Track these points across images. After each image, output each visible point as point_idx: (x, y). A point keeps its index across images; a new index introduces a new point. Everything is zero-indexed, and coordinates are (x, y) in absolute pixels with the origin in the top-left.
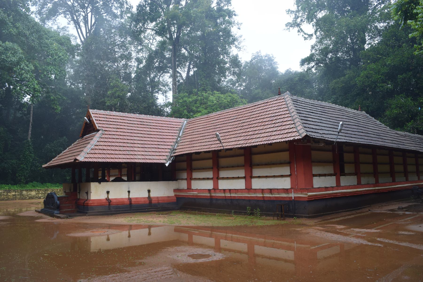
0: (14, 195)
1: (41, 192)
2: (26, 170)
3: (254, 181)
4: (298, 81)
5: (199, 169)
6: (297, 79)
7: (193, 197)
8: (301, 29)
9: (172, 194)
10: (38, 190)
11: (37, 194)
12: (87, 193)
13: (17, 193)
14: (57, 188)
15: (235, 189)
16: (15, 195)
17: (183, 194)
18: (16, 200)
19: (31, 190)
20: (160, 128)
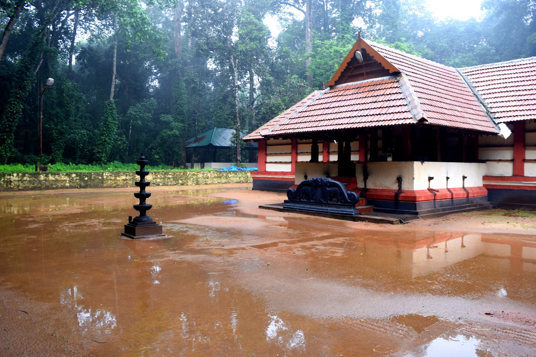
0: (124, 180)
1: (159, 176)
2: (109, 144)
4: (464, 32)
6: (462, 29)
9: (480, 183)
11: (154, 179)
12: (399, 180)
13: (128, 178)
14: (180, 170)
16: (126, 180)
17: (510, 184)
18: (127, 187)
20: (442, 77)
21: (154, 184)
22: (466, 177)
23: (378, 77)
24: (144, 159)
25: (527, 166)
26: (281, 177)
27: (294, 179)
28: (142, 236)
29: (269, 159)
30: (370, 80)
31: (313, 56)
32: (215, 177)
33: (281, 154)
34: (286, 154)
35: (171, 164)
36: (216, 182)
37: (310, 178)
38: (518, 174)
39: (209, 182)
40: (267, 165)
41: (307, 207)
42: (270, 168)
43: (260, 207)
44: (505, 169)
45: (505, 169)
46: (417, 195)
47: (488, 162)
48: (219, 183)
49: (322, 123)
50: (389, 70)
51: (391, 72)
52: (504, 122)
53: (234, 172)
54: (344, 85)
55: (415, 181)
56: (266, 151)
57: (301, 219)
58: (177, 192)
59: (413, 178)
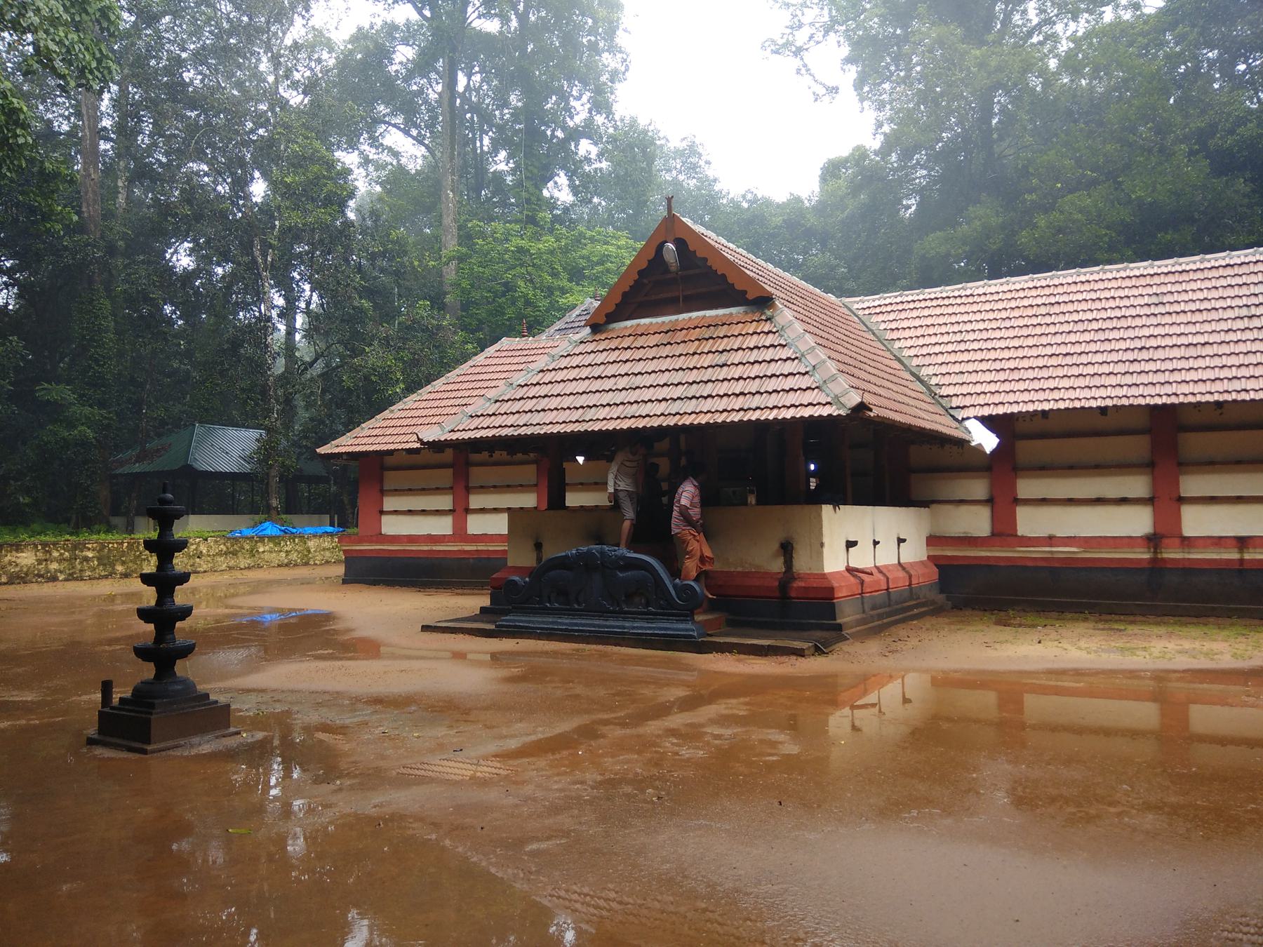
1: (55, 554)
3: (1022, 513)
5: (1071, 467)
6: (778, 220)
7: (1044, 564)
8: (805, 66)
10: (45, 545)
11: (40, 562)
12: (787, 549)
15: (1106, 538)
17: (988, 554)
19: (18, 547)
21: (41, 576)
22: (904, 541)
23: (717, 308)
24: (170, 502)
25: (1022, 513)
26: (426, 548)
27: (505, 551)
28: (170, 743)
29: (390, 503)
30: (694, 314)
31: (461, 259)
32: (220, 554)
33: (424, 491)
34: (437, 490)
35: (68, 521)
36: (224, 567)
37: (550, 552)
38: (1004, 531)
39: (205, 567)
40: (384, 519)
41: (565, 622)
42: (391, 526)
43: (426, 628)
44: (977, 522)
45: (977, 522)
46: (835, 585)
47: (934, 506)
48: (231, 568)
49: (590, 414)
50: (745, 292)
51: (750, 296)
52: (976, 417)
53: (271, 538)
54: (629, 323)
55: (826, 550)
56: (467, 481)
57: (555, 654)
58: (111, 598)
59: (822, 545)
